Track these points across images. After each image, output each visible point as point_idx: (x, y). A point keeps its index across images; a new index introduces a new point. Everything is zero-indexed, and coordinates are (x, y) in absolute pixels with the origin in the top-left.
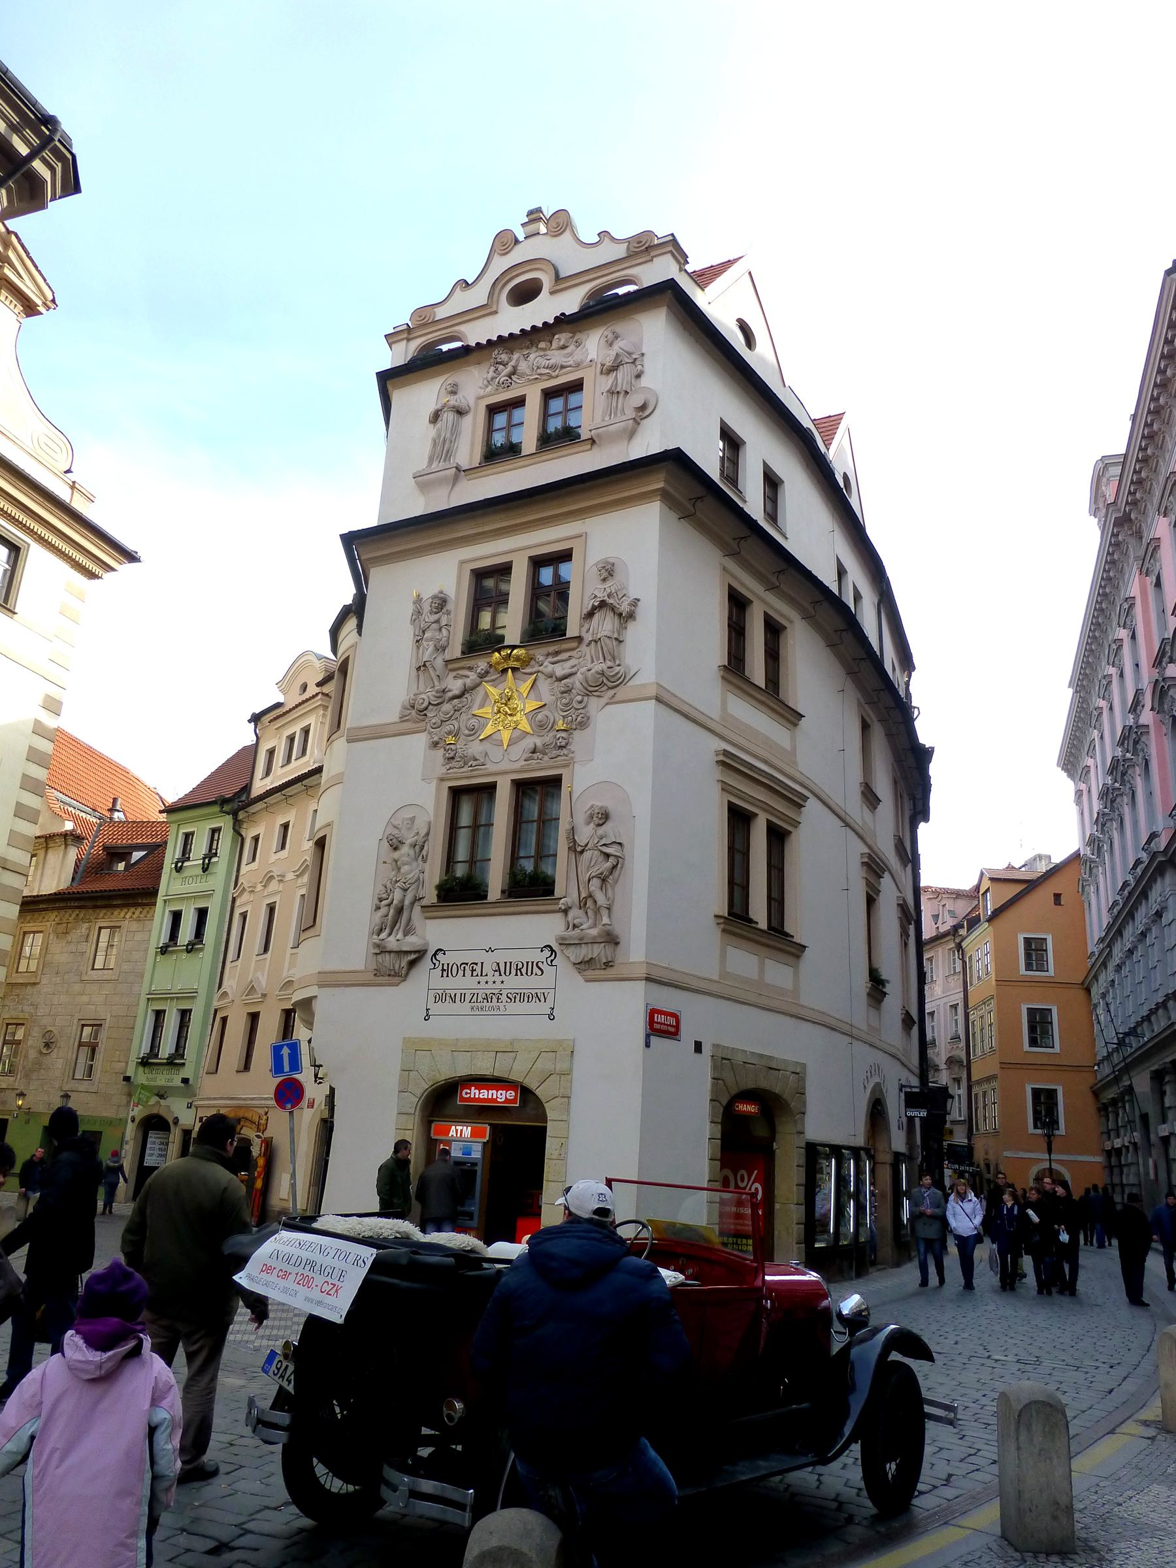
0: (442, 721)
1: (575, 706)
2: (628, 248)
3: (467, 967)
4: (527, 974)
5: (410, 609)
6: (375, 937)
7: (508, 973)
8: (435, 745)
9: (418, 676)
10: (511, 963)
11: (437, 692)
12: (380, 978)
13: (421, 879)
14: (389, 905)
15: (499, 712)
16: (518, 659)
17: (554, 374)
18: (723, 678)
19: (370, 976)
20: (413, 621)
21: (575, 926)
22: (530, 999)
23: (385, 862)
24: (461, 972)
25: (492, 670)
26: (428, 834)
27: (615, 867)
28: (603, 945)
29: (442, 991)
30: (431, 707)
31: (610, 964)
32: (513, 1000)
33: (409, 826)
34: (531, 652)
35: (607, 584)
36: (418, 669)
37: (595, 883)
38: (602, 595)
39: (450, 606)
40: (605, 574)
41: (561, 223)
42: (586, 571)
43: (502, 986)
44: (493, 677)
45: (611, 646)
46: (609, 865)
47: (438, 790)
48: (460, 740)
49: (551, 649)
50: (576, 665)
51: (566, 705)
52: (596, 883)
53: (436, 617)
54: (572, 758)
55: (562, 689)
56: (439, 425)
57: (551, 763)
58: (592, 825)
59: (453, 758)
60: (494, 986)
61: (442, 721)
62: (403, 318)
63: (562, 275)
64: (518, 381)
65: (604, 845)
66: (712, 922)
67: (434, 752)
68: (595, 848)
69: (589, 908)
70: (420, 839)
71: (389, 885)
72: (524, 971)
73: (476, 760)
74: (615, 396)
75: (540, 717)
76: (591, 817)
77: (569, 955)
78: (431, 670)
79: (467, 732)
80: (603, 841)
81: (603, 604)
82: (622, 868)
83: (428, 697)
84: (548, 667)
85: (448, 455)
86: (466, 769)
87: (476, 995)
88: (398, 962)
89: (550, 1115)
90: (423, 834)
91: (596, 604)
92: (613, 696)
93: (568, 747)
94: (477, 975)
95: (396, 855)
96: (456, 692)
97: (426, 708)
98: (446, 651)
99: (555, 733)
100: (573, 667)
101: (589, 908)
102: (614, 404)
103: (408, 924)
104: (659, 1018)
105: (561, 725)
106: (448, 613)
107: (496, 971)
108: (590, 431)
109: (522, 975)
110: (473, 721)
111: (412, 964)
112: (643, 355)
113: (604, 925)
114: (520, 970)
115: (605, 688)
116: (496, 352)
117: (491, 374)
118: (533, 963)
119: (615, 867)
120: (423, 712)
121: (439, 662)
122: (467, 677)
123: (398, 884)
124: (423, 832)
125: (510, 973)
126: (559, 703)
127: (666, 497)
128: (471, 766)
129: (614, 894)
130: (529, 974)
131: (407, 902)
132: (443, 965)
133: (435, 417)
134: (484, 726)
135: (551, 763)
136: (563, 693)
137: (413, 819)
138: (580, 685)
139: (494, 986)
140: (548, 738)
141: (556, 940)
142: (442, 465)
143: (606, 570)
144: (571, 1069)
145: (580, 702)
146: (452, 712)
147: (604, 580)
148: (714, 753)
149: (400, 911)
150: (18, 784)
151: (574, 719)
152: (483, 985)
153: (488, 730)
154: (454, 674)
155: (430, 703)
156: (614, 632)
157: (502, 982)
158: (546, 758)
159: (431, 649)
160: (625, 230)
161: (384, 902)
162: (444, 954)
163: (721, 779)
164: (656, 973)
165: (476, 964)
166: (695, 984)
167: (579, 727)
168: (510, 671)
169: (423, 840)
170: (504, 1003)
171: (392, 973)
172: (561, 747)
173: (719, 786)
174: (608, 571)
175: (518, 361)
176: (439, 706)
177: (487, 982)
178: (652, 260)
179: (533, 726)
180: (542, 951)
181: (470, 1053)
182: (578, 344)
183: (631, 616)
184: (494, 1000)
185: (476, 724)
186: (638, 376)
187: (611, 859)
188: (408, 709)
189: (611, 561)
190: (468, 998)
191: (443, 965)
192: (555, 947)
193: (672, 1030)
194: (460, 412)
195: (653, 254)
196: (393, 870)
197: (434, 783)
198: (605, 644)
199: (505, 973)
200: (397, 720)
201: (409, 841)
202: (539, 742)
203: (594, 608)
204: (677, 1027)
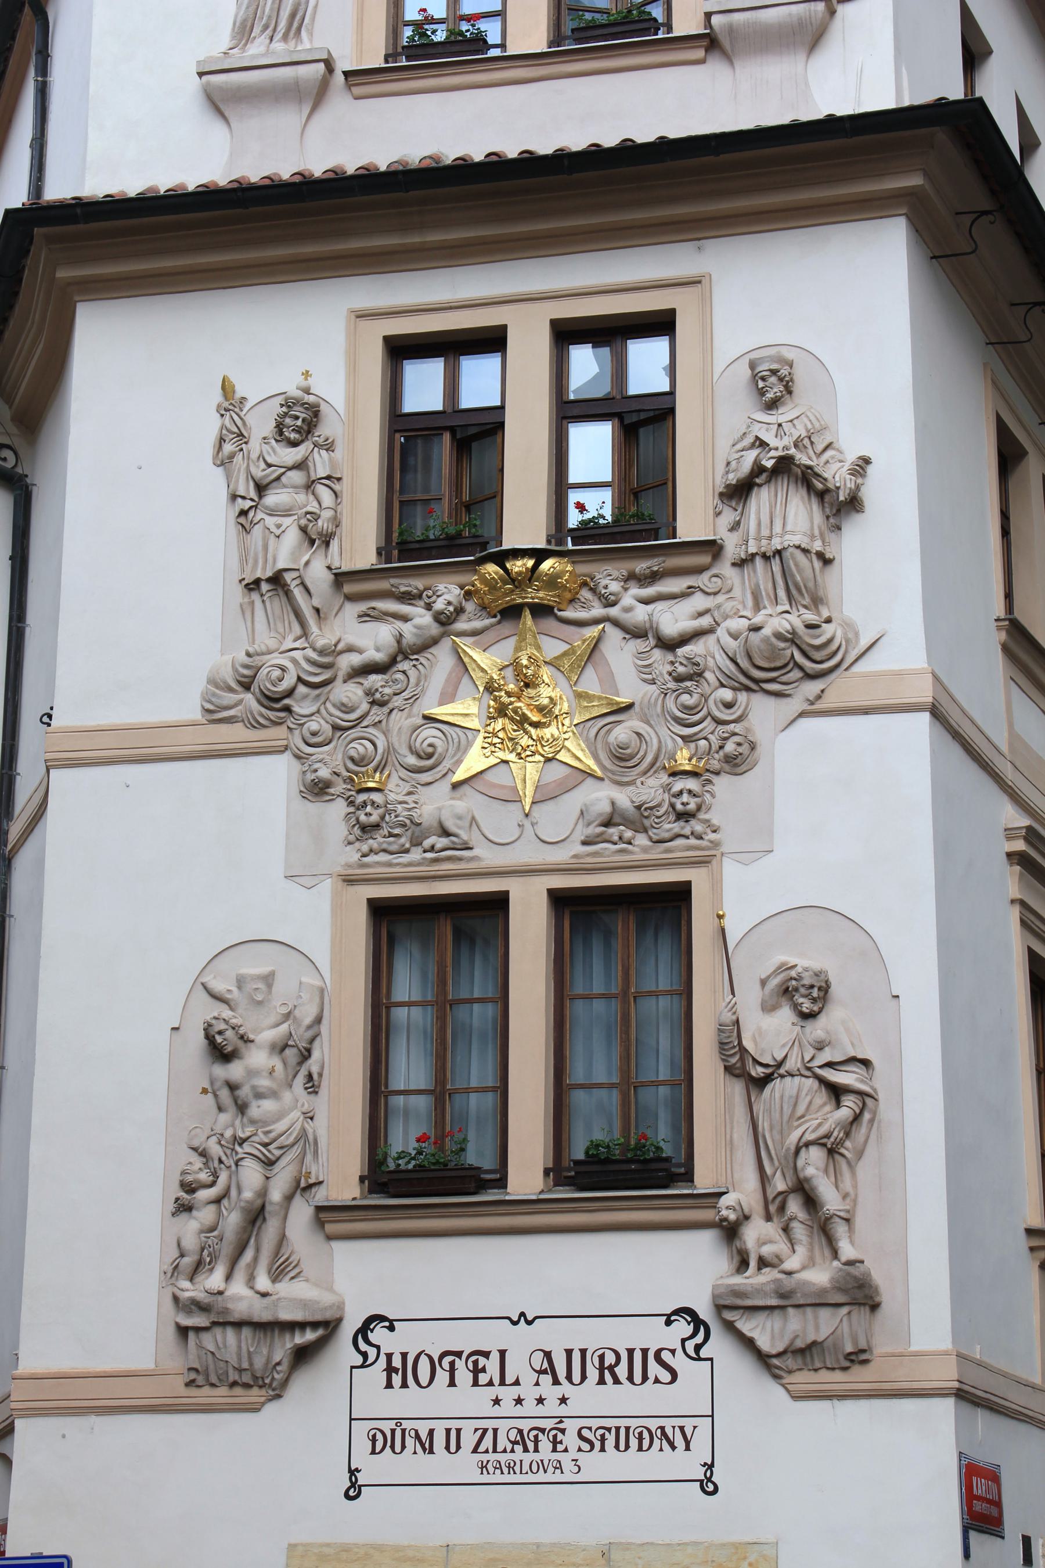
0: (336, 728)
1: (717, 713)
3: (460, 1364)
4: (630, 1378)
5: (212, 425)
6: (185, 1284)
7: (576, 1376)
8: (318, 789)
9: (253, 602)
10: (583, 1352)
11: (321, 652)
12: (207, 1390)
13: (311, 1137)
14: (218, 1201)
15: (502, 711)
16: (552, 582)
18: (1005, 648)
19: (176, 1386)
20: (224, 462)
22: (646, 1443)
23: (205, 1091)
24: (442, 1376)
25: (470, 606)
26: (318, 1020)
27: (857, 1118)
28: (844, 1310)
29: (392, 1424)
30: (302, 689)
31: (863, 1357)
32: (598, 1445)
33: (259, 998)
34: (583, 569)
35: (784, 414)
36: (253, 586)
37: (812, 1163)
38: (780, 445)
39: (328, 428)
40: (775, 390)
42: (715, 381)
43: (563, 1411)
44: (478, 624)
45: (809, 573)
46: (844, 1113)
47: (337, 908)
48: (394, 776)
49: (641, 566)
50: (707, 611)
51: (688, 709)
52: (815, 1155)
53: (291, 455)
54: (716, 844)
55: (681, 669)
57: (657, 853)
58: (785, 1015)
59: (377, 826)
60: (541, 1410)
61: (336, 728)
65: (830, 1065)
66: (1023, 1243)
67: (315, 808)
68: (808, 1070)
69: (791, 1219)
70: (301, 1038)
71: (215, 1150)
72: (622, 1371)
73: (446, 833)
75: (621, 733)
76: (787, 992)
77: (754, 1334)
78: (298, 593)
79: (412, 760)
80: (826, 1056)
81: (784, 466)
82: (872, 1121)
83: (294, 661)
85: (296, 25)
86: (416, 855)
87: (490, 1435)
88: (265, 1351)
90: (308, 1020)
91: (769, 464)
92: (819, 697)
93: (702, 816)
94: (490, 1383)
95: (235, 1071)
98: (334, 544)
99: (664, 778)
100: (701, 614)
101: (791, 1219)
103: (277, 1253)
104: (980, 1487)
105: (683, 759)
106: (329, 447)
107: (545, 1372)
108: (708, 15)
109: (617, 1381)
110: (429, 734)
111: (303, 1355)
113: (850, 1263)
114: (611, 1368)
115: (796, 674)
118: (645, 1352)
119: (857, 1118)
121: (318, 574)
122: (405, 619)
123: (247, 1148)
124: (307, 1013)
125: (584, 1377)
128: (433, 847)
129: (855, 1186)
130: (638, 1377)
131: (276, 1195)
132: (389, 1356)
134: (462, 749)
135: (657, 853)
136: (679, 679)
137: (268, 980)
138: (728, 662)
139: (541, 1410)
141: (715, 1297)
142: (280, 50)
143: (781, 379)
145: (729, 705)
146: (365, 706)
147: (772, 405)
148: (1001, 834)
151: (715, 747)
152: (508, 1407)
153: (474, 761)
154: (363, 607)
155: (299, 679)
156: (812, 537)
157: (563, 1400)
158: (641, 840)
159: (292, 536)
161: (203, 1194)
162: (391, 1328)
163: (1019, 896)
164: (980, 1382)
165: (486, 1355)
166: (1017, 1398)
167: (727, 767)
168: (527, 613)
169: (309, 1034)
170: (573, 1453)
171: (246, 1378)
172: (684, 816)
173: (1015, 913)
177: (519, 1401)
179: (603, 756)
180: (668, 1323)
183: (854, 503)
184: (545, 1445)
185: (438, 743)
187: (850, 1102)
188: (231, 690)
189: (789, 354)
190: (469, 1440)
191: (389, 1356)
192: (705, 1312)
193: (994, 1512)
196: (220, 1109)
197: (327, 885)
198: (796, 565)
199: (569, 1377)
200: (197, 715)
201: (269, 1035)
202: (624, 798)
203: (758, 469)
204: (998, 1504)
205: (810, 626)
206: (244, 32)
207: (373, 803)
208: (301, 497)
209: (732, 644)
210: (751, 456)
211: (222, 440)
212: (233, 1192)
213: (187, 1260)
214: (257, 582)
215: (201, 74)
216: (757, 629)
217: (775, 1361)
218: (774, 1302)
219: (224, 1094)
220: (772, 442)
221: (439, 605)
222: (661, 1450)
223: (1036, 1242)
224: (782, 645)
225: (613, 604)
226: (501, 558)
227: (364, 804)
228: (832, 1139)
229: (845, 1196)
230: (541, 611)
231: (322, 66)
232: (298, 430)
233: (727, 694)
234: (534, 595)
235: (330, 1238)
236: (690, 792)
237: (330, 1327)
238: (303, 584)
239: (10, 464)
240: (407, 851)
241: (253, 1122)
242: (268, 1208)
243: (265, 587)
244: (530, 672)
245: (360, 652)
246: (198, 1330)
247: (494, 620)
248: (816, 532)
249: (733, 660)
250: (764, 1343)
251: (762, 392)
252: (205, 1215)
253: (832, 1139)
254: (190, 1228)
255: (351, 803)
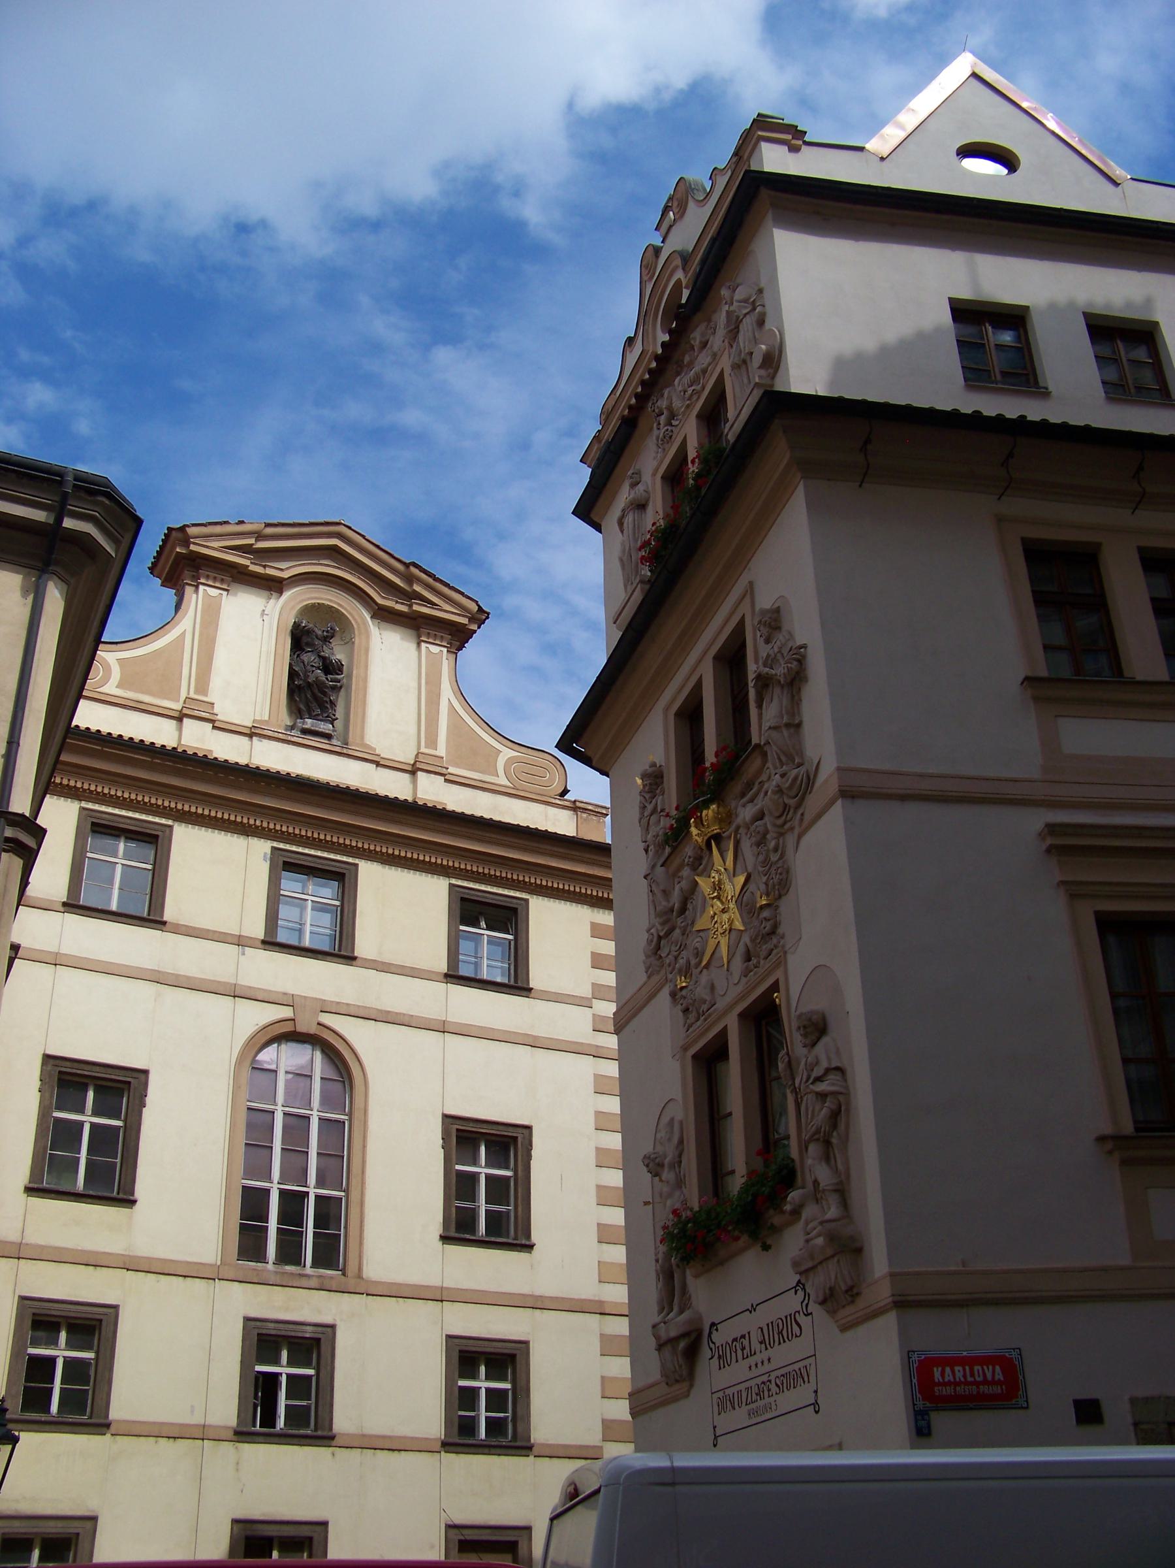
10: (772, 1323)
17: (698, 388)
28: (836, 1259)
64: (677, 423)
74: (743, 368)
94: (747, 1357)
112: (761, 291)
127: (809, 469)
134: (705, 943)
143: (765, 625)
150: (593, 1200)
175: (670, 398)
187: (829, 1103)
215: (615, 623)
218: (810, 1264)
222: (801, 1385)
228: (822, 1134)
229: (836, 1171)
236: (765, 919)
248: (784, 712)
253: (822, 1134)
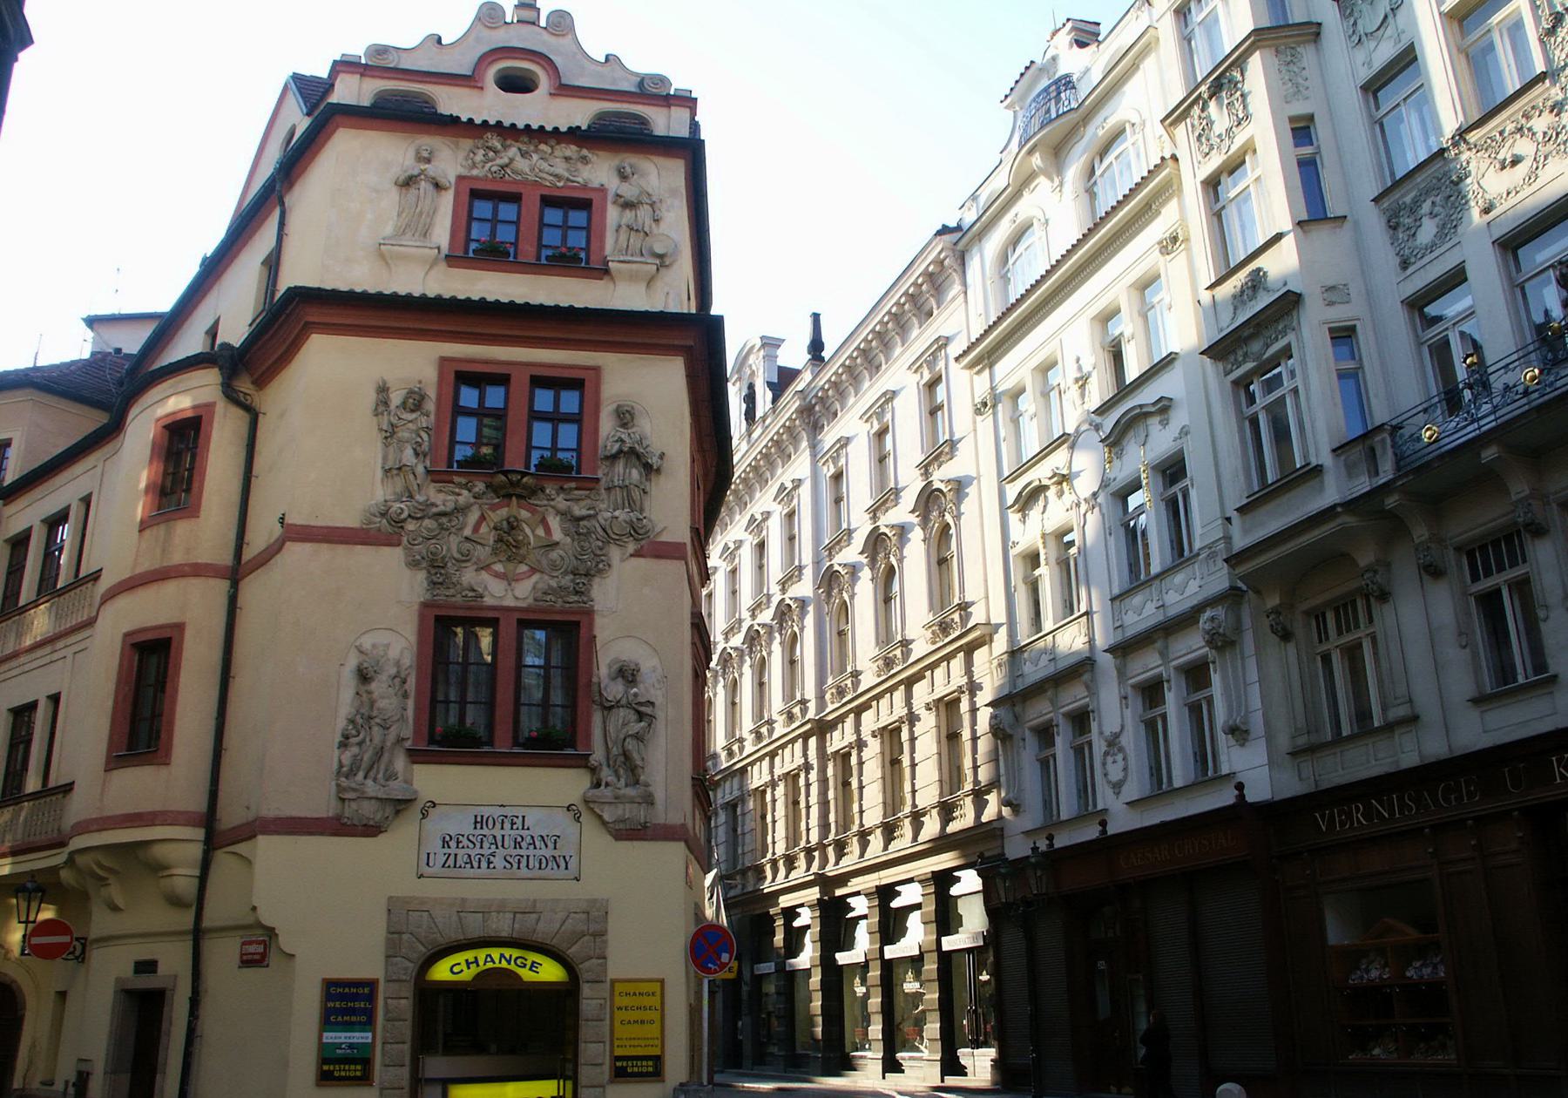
2: (641, 84)
5: (371, 397)
6: (344, 779)
8: (413, 564)
11: (420, 503)
14: (360, 744)
16: (525, 487)
21: (607, 785)
26: (410, 666)
30: (409, 520)
41: (562, 23)
54: (592, 606)
56: (413, 191)
59: (441, 584)
62: (357, 49)
63: (564, 81)
65: (640, 704)
73: (474, 590)
75: (554, 555)
84: (561, 502)
89: (584, 976)
96: (442, 508)
97: (404, 521)
99: (572, 577)
102: (632, 240)
103: (387, 770)
111: (398, 812)
116: (489, 135)
117: (479, 157)
119: (650, 725)
120: (398, 523)
121: (420, 469)
122: (459, 495)
123: (377, 720)
126: (576, 543)
128: (466, 596)
131: (388, 744)
133: (408, 183)
136: (578, 534)
137: (388, 646)
140: (567, 581)
144: (606, 931)
149: (380, 753)
159: (409, 452)
160: (640, 62)
174: (625, 417)
176: (420, 521)
178: (669, 106)
181: (481, 915)
182: (585, 160)
183: (658, 471)
186: (657, 221)
194: (438, 186)
195: (671, 102)
202: (553, 583)
203: (620, 451)
205: (638, 519)
206: (401, 232)
207: (441, 574)
208: (414, 436)
209: (602, 522)
210: (617, 446)
211: (377, 405)
212: (368, 739)
213: (345, 769)
214: (390, 469)
216: (617, 518)
217: (611, 825)
219: (364, 695)
220: (627, 440)
221: (477, 489)
223: (696, 782)
224: (625, 525)
225: (553, 500)
226: (505, 473)
227: (436, 573)
230: (519, 497)
231: (436, 251)
232: (415, 405)
233: (600, 544)
234: (518, 491)
235: (415, 762)
237: (408, 802)
238: (414, 474)
239: (248, 402)
240: (453, 596)
241: (378, 709)
242: (386, 748)
243: (395, 472)
244: (515, 524)
245: (437, 506)
246: (350, 800)
247: (497, 500)
249: (604, 530)
250: (606, 817)
251: (622, 420)
252: (355, 750)
254: (347, 758)
255: (429, 572)
